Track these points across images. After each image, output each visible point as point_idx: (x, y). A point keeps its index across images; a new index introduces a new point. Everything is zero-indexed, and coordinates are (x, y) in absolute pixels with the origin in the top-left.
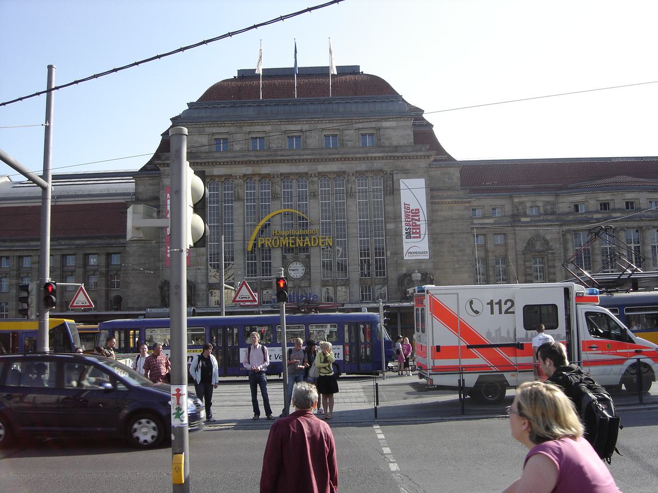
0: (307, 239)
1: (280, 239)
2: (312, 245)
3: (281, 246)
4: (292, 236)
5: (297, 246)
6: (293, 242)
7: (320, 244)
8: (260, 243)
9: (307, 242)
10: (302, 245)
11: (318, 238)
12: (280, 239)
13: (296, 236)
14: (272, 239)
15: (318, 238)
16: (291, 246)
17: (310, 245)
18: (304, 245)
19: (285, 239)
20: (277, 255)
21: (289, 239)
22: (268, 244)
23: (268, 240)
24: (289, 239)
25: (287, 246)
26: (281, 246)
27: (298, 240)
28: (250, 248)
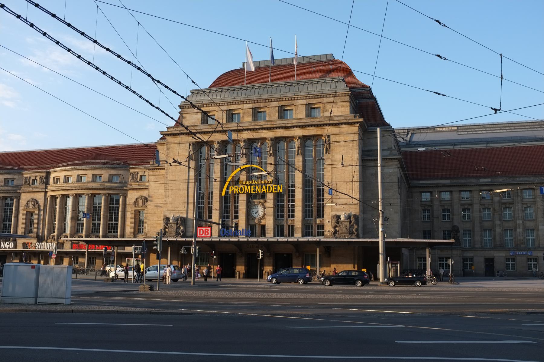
0: (264, 187)
1: (244, 187)
2: (268, 192)
3: (245, 192)
4: (254, 185)
5: (257, 192)
6: (254, 189)
7: (273, 191)
8: (230, 190)
9: (264, 189)
10: (260, 192)
11: (272, 186)
12: (244, 187)
13: (256, 184)
14: (239, 187)
15: (272, 186)
16: (252, 192)
17: (266, 192)
18: (262, 192)
19: (248, 187)
20: (243, 199)
21: (251, 187)
22: (236, 191)
23: (236, 188)
24: (251, 187)
25: (250, 192)
26: (245, 192)
27: (257, 187)
28: (223, 194)
